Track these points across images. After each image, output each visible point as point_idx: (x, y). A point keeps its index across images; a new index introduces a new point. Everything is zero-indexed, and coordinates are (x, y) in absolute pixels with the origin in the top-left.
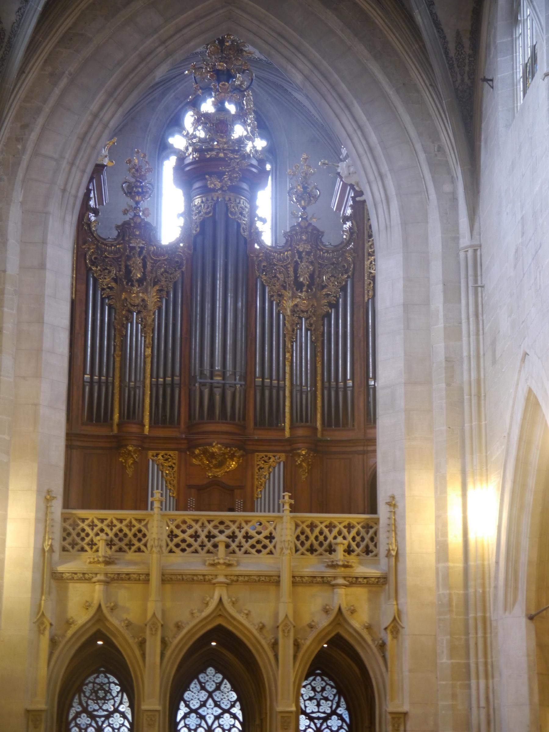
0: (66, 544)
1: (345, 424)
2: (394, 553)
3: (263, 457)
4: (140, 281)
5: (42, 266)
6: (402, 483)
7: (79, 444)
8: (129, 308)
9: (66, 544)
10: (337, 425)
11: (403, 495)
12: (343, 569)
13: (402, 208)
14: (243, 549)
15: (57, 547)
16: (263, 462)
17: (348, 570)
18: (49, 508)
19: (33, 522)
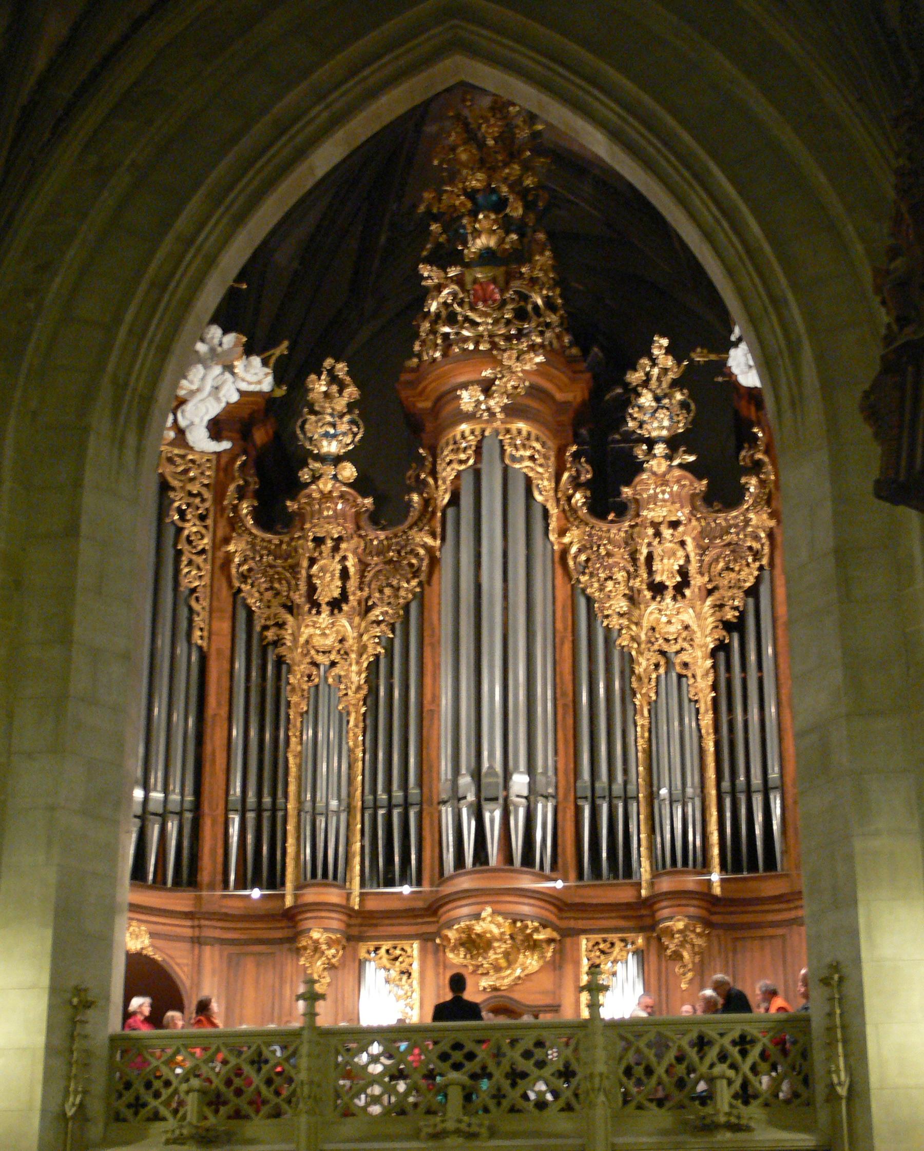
0: (120, 1105)
1: (770, 863)
2: (842, 1091)
3: (597, 943)
4: (336, 605)
5: (72, 531)
6: (854, 934)
7: (217, 934)
8: (312, 658)
9: (120, 1105)
10: (753, 867)
11: (857, 961)
12: (729, 1135)
13: (820, 358)
14: (506, 1103)
15: (97, 1108)
16: (598, 953)
17: (740, 1136)
18: (78, 1026)
19: (40, 1054)
